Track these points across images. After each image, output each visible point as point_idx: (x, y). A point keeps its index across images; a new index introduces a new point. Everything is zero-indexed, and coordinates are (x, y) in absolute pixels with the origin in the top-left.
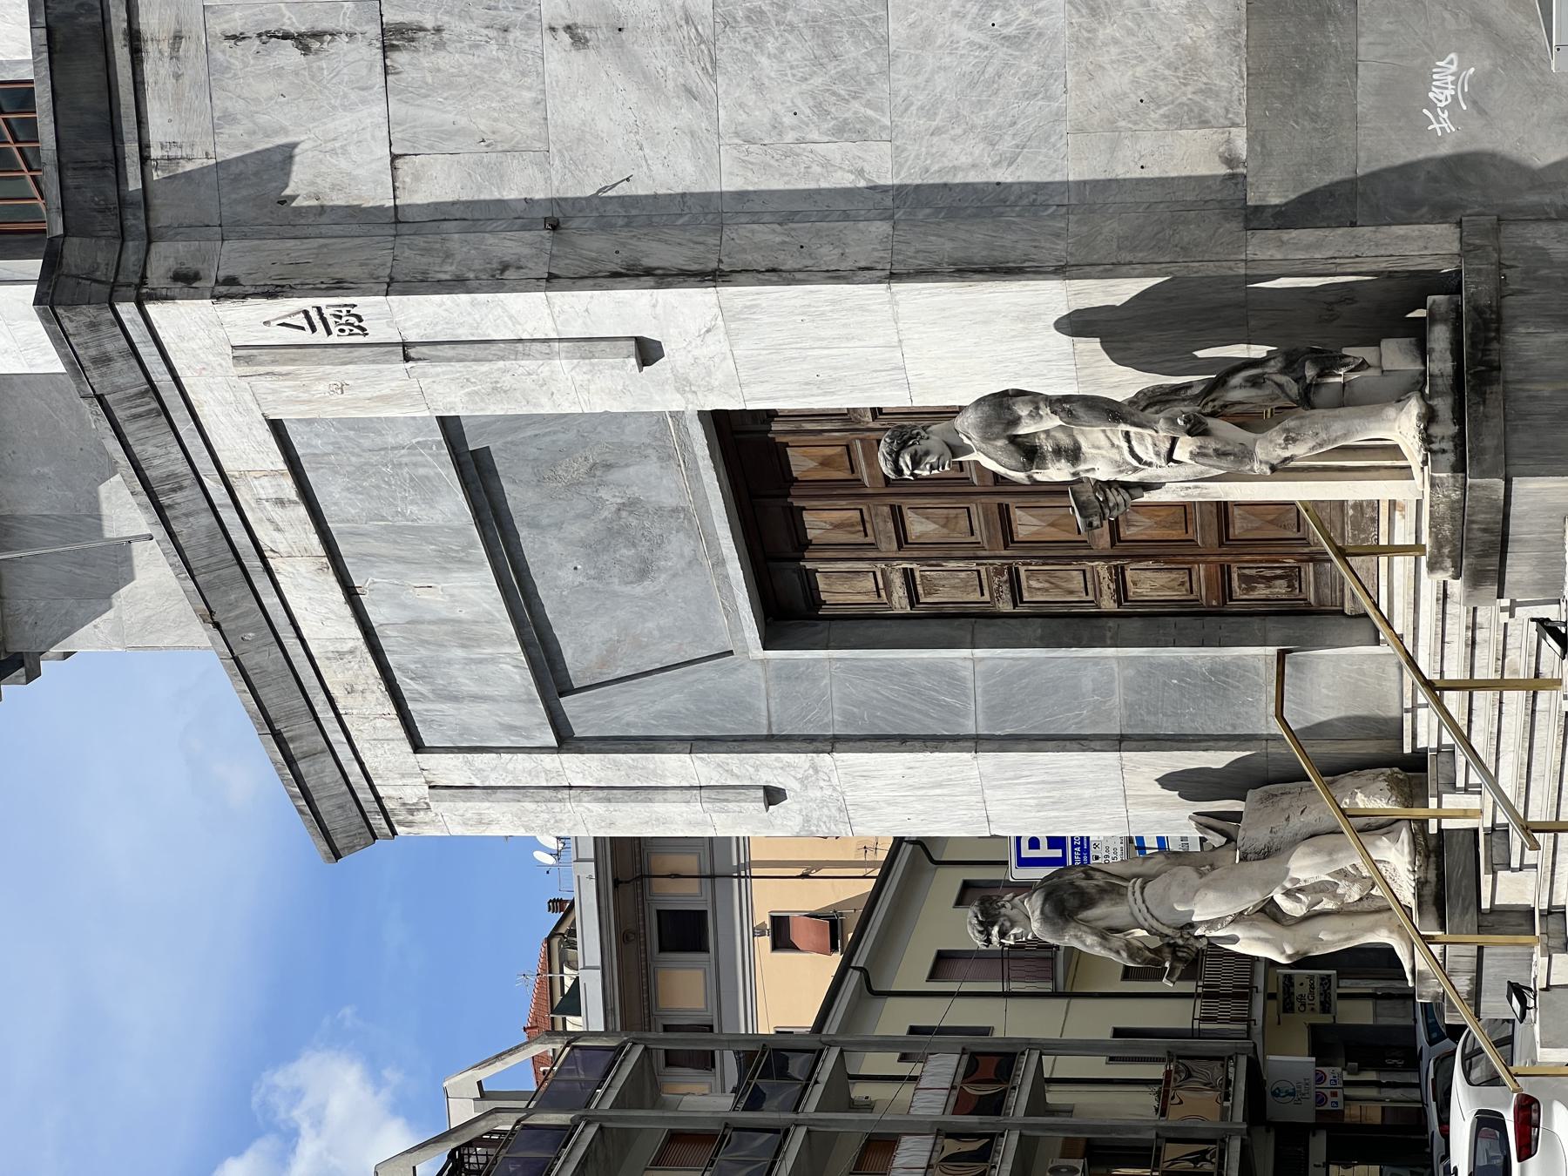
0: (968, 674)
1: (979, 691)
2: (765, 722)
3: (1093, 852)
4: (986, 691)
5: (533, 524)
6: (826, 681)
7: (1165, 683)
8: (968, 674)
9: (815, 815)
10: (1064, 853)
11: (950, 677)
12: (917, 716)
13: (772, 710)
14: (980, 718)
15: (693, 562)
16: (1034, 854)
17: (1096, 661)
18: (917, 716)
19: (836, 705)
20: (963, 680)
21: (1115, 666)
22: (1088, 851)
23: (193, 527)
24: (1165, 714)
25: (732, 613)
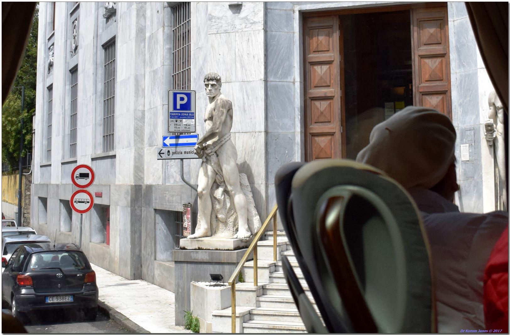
0: (289, 80)
1: (283, 83)
2: (272, 8)
3: (179, 120)
4: (283, 86)
6: (286, 30)
7: (286, 148)
8: (289, 80)
9: (223, 21)
10: (178, 110)
11: (288, 72)
12: (274, 61)
13: (276, 11)
14: (274, 83)
16: (178, 99)
17: (294, 124)
18: (274, 61)
19: (278, 33)
20: (287, 78)
21: (292, 131)
22: (179, 118)
24: (275, 148)
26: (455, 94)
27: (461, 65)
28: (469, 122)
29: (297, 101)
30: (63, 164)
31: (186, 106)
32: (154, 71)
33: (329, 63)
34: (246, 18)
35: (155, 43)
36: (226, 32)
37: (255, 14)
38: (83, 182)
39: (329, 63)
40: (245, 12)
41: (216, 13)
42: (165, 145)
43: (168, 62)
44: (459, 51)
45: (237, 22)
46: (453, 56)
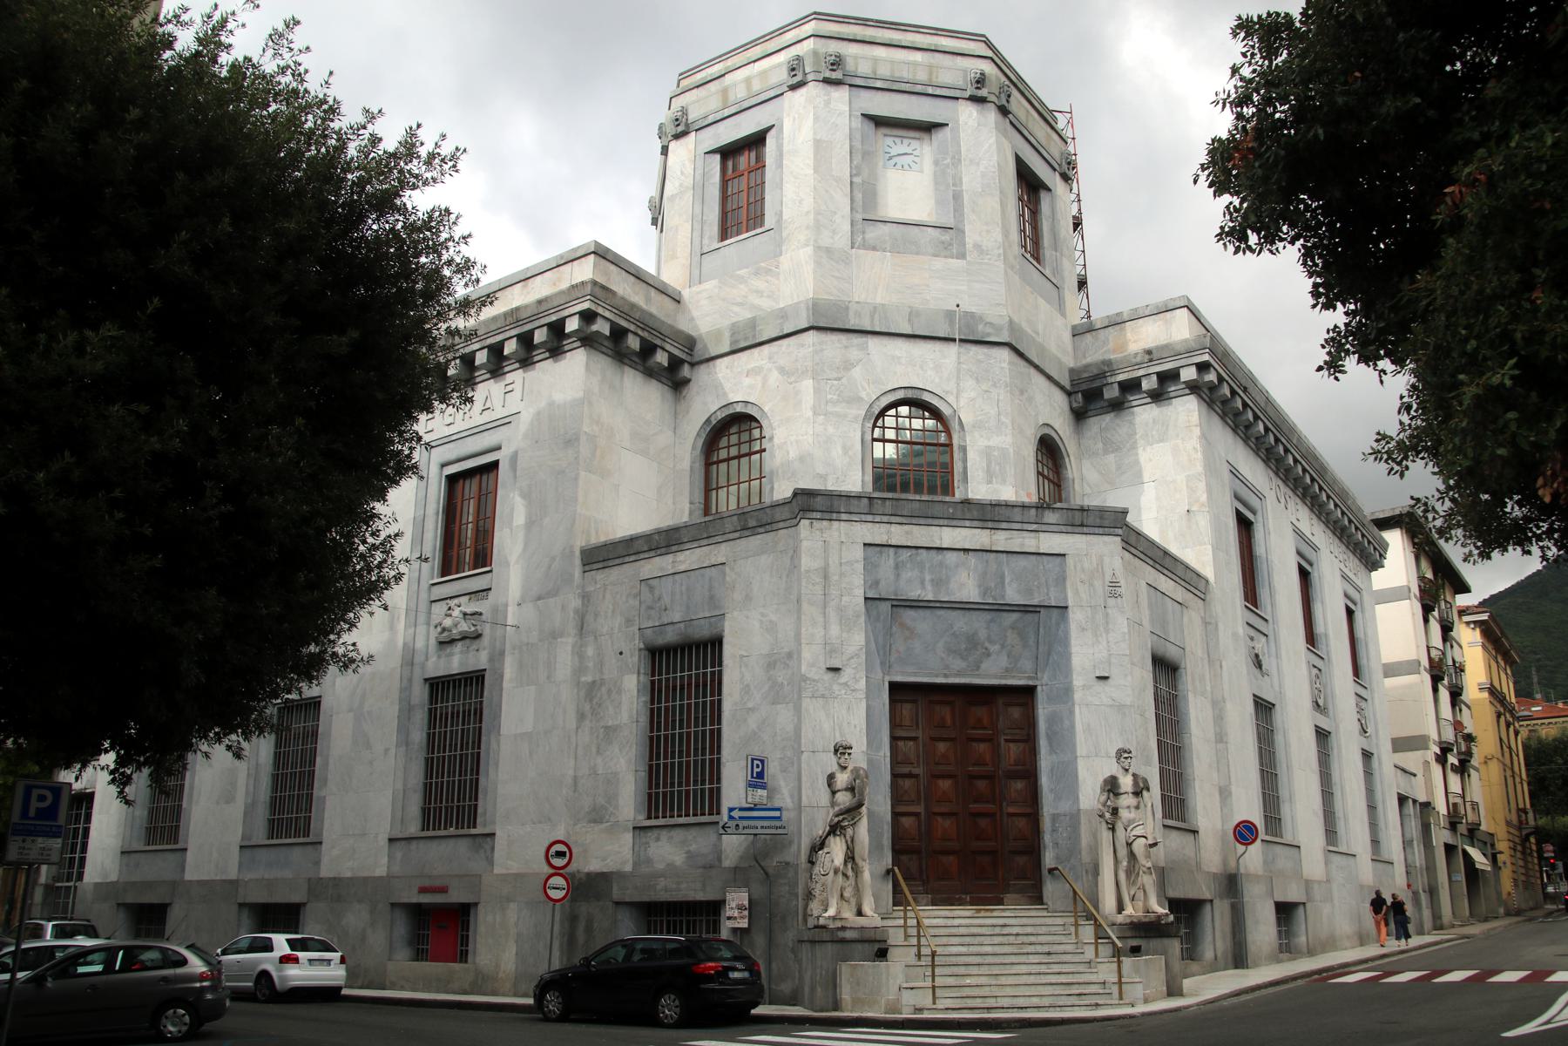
5: (992, 621)
15: (947, 667)
23: (1017, 514)
25: (915, 674)
26: (1045, 781)
27: (1052, 750)
28: (1064, 807)
29: (888, 778)
30: (391, 840)
31: (761, 775)
32: (606, 728)
33: (914, 739)
34: (846, 684)
35: (609, 691)
36: (823, 696)
37: (857, 681)
38: (558, 862)
39: (914, 739)
40: (845, 676)
41: (813, 673)
42: (731, 818)
43: (644, 720)
44: (1049, 738)
45: (835, 687)
46: (1043, 743)
